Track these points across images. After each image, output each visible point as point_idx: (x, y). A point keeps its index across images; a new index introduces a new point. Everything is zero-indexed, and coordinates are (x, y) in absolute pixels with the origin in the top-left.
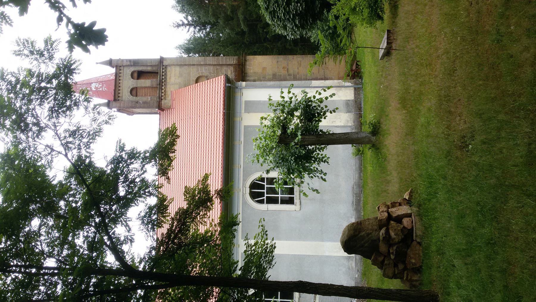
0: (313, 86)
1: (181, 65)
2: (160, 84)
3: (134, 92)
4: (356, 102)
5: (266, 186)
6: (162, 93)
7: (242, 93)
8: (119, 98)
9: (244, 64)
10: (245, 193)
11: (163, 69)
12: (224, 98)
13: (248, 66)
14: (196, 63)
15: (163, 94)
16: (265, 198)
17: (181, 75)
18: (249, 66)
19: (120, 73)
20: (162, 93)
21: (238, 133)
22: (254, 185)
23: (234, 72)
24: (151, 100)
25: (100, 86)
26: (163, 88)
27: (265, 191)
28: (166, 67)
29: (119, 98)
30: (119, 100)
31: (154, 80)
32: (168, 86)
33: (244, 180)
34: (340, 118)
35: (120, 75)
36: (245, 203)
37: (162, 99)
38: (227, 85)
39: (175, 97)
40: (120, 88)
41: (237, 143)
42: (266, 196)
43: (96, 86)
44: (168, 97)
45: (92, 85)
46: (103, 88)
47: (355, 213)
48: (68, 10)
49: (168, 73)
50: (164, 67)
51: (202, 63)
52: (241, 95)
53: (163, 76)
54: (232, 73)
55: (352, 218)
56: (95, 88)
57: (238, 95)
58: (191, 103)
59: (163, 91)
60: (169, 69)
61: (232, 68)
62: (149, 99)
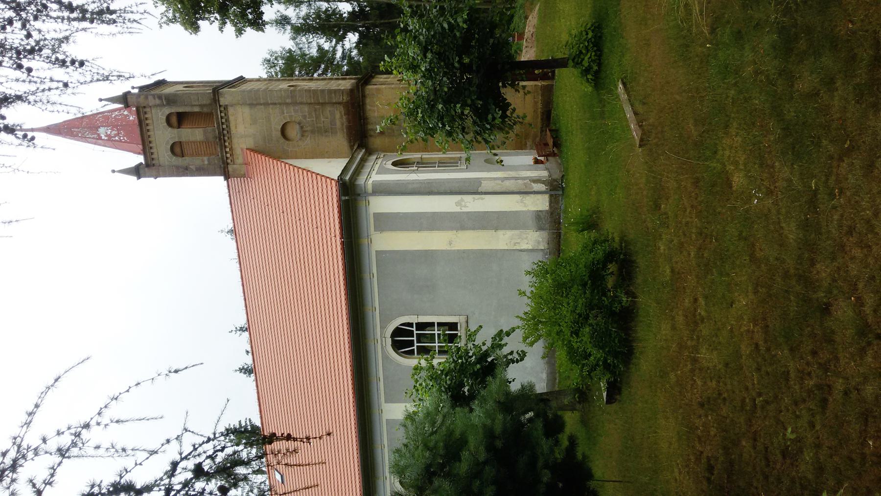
0: (483, 191)
1: (252, 105)
2: (220, 139)
3: (177, 150)
4: (552, 214)
5: (415, 332)
6: (226, 153)
7: (367, 201)
8: (154, 162)
9: (361, 104)
10: (384, 345)
11: (221, 112)
12: (340, 217)
13: (370, 106)
14: (277, 102)
15: (228, 155)
16: (415, 348)
17: (254, 121)
18: (372, 106)
19: (146, 119)
20: (226, 153)
21: (368, 262)
22: (397, 332)
23: (345, 114)
24: (209, 164)
25: (114, 132)
26: (227, 144)
27: (415, 339)
28: (226, 107)
29: (154, 162)
30: (154, 165)
31: (209, 129)
32: (235, 141)
33: (383, 328)
34: (526, 238)
35: (147, 122)
36: (385, 357)
37: (228, 164)
38: (343, 198)
39: (249, 158)
40: (151, 145)
41: (366, 276)
42: (417, 346)
43: (106, 133)
44: (238, 158)
45: (99, 130)
46: (121, 137)
47: (546, 366)
48: (54, 149)
49: (231, 118)
50: (222, 109)
51: (288, 101)
52: (367, 205)
53: (223, 123)
54: (341, 116)
55: (542, 373)
56: (106, 136)
57: (362, 204)
58: (305, 385)
59: (228, 150)
60: (231, 111)
61: (341, 108)
62: (206, 162)
